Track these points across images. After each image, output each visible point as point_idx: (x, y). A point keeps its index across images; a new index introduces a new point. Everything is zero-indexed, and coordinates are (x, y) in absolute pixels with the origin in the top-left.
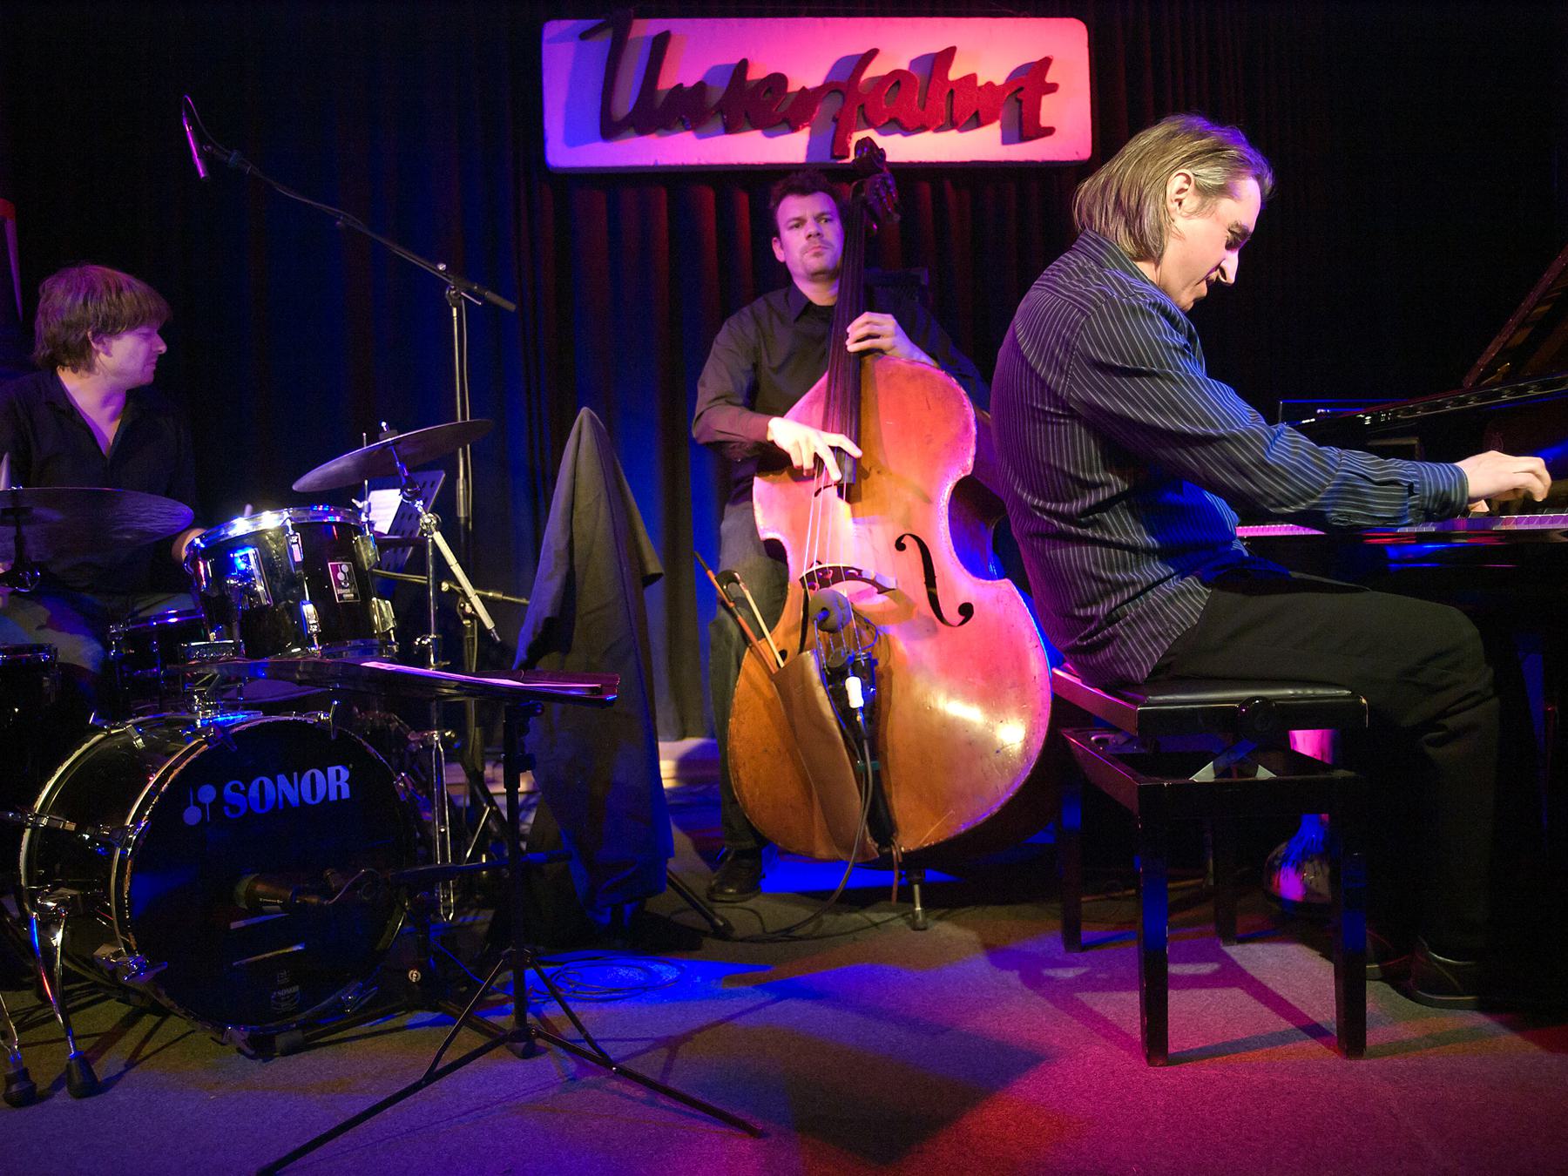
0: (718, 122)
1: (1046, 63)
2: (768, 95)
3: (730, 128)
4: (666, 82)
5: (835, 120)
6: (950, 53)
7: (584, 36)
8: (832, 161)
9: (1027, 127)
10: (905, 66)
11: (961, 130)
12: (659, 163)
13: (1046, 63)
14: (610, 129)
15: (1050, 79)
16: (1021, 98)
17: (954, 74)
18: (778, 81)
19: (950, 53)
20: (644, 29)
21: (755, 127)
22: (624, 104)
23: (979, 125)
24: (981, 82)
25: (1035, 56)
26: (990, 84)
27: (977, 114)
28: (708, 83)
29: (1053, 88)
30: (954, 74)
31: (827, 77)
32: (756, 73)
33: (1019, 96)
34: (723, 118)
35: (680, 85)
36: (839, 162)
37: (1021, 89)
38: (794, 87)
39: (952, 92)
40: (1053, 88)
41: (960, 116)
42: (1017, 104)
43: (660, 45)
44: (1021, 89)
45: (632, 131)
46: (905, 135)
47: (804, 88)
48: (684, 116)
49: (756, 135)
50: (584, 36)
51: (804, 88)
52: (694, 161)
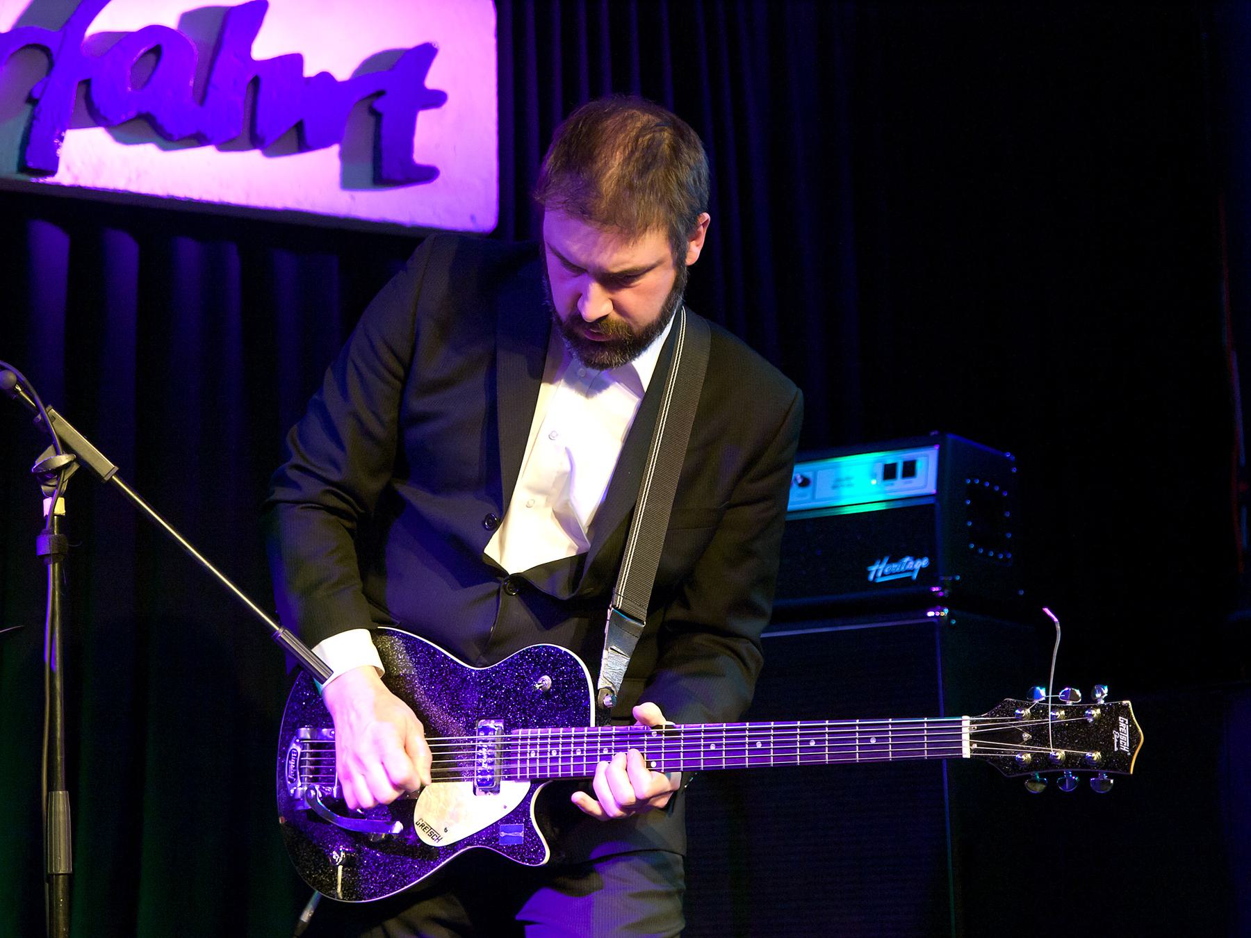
1: (425, 54)
5: (31, 100)
8: (23, 177)
10: (171, 22)
13: (425, 54)
15: (432, 81)
17: (265, 47)
23: (304, 145)
24: (310, 71)
25: (409, 41)
26: (325, 77)
29: (437, 99)
30: (265, 47)
31: (22, 18)
36: (41, 180)
37: (380, 94)
39: (256, 81)
40: (437, 99)
44: (380, 94)
46: (164, 149)
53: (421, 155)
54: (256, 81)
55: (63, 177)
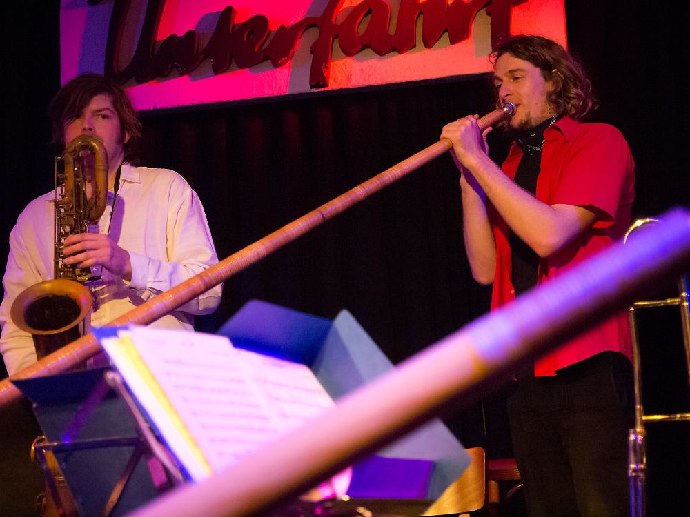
0: (208, 64)
4: (162, 35)
18: (259, 23)
32: (239, 19)
38: (273, 27)
47: (282, 26)
48: (176, 63)
51: (283, 27)
55: (333, 85)
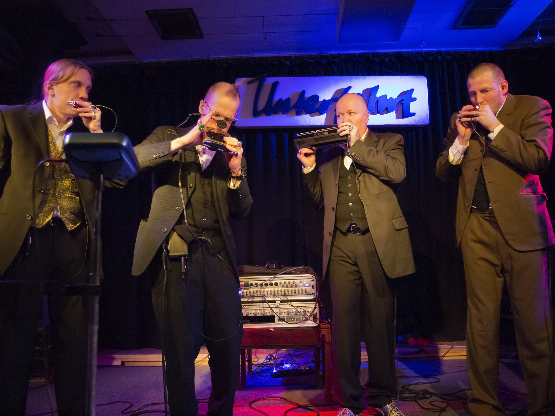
0: (294, 111)
1: (412, 90)
2: (312, 102)
3: (298, 113)
4: (276, 99)
6: (377, 87)
7: (249, 83)
9: (405, 113)
11: (381, 114)
12: (273, 126)
13: (412, 90)
14: (256, 113)
15: (413, 96)
16: (403, 103)
17: (378, 95)
19: (377, 87)
20: (270, 81)
21: (307, 113)
22: (262, 105)
23: (388, 112)
24: (388, 98)
26: (391, 98)
27: (387, 108)
28: (291, 98)
29: (415, 99)
30: (378, 95)
32: (308, 95)
33: (402, 102)
34: (296, 110)
35: (281, 99)
37: (402, 100)
38: (321, 99)
39: (377, 101)
40: (415, 99)
41: (380, 109)
42: (402, 105)
43: (275, 85)
45: (264, 114)
47: (325, 100)
48: (282, 109)
49: (308, 115)
50: (249, 83)
52: (286, 125)
53: (412, 111)
54: (377, 101)
